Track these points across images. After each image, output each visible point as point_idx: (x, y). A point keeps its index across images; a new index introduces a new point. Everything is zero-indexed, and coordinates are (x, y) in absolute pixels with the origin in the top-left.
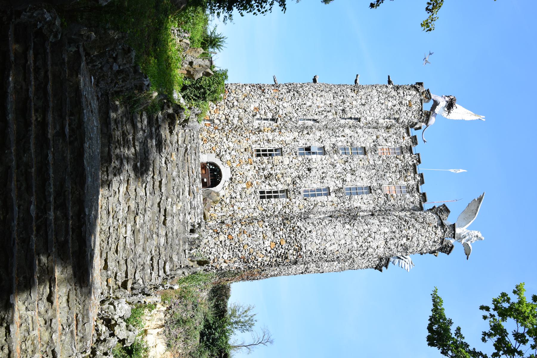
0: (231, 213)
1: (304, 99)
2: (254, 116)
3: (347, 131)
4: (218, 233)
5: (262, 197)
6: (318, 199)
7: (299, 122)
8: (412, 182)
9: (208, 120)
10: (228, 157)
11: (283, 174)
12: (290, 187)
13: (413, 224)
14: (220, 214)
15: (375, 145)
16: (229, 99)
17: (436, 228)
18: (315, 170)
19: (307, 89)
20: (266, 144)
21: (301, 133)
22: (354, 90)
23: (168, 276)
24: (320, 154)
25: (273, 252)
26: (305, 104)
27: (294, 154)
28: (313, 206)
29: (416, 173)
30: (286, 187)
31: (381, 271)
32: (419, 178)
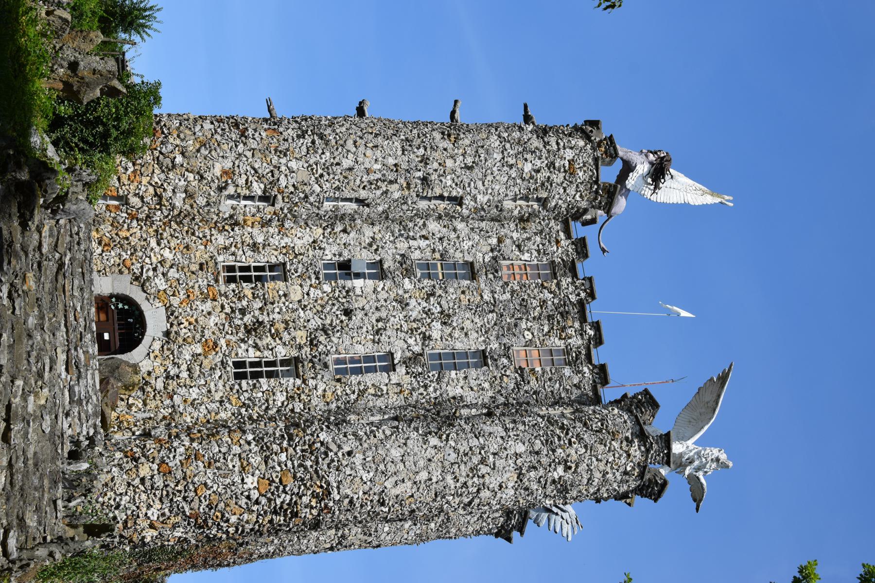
0: (166, 412)
1: (336, 153)
2: (220, 189)
3: (433, 226)
4: (136, 460)
5: (239, 376)
6: (369, 379)
7: (326, 203)
8: (576, 341)
9: (113, 198)
10: (160, 283)
11: (286, 323)
12: (303, 352)
13: (578, 435)
14: (140, 416)
15: (494, 258)
16: (164, 150)
17: (630, 442)
18: (360, 314)
19: (344, 129)
20: (249, 253)
21: (329, 230)
22: (449, 135)
23: (13, 562)
24: (372, 277)
25: (263, 501)
26: (338, 164)
27: (313, 277)
28: (356, 396)
29: (585, 321)
31: (509, 540)
32: (592, 333)
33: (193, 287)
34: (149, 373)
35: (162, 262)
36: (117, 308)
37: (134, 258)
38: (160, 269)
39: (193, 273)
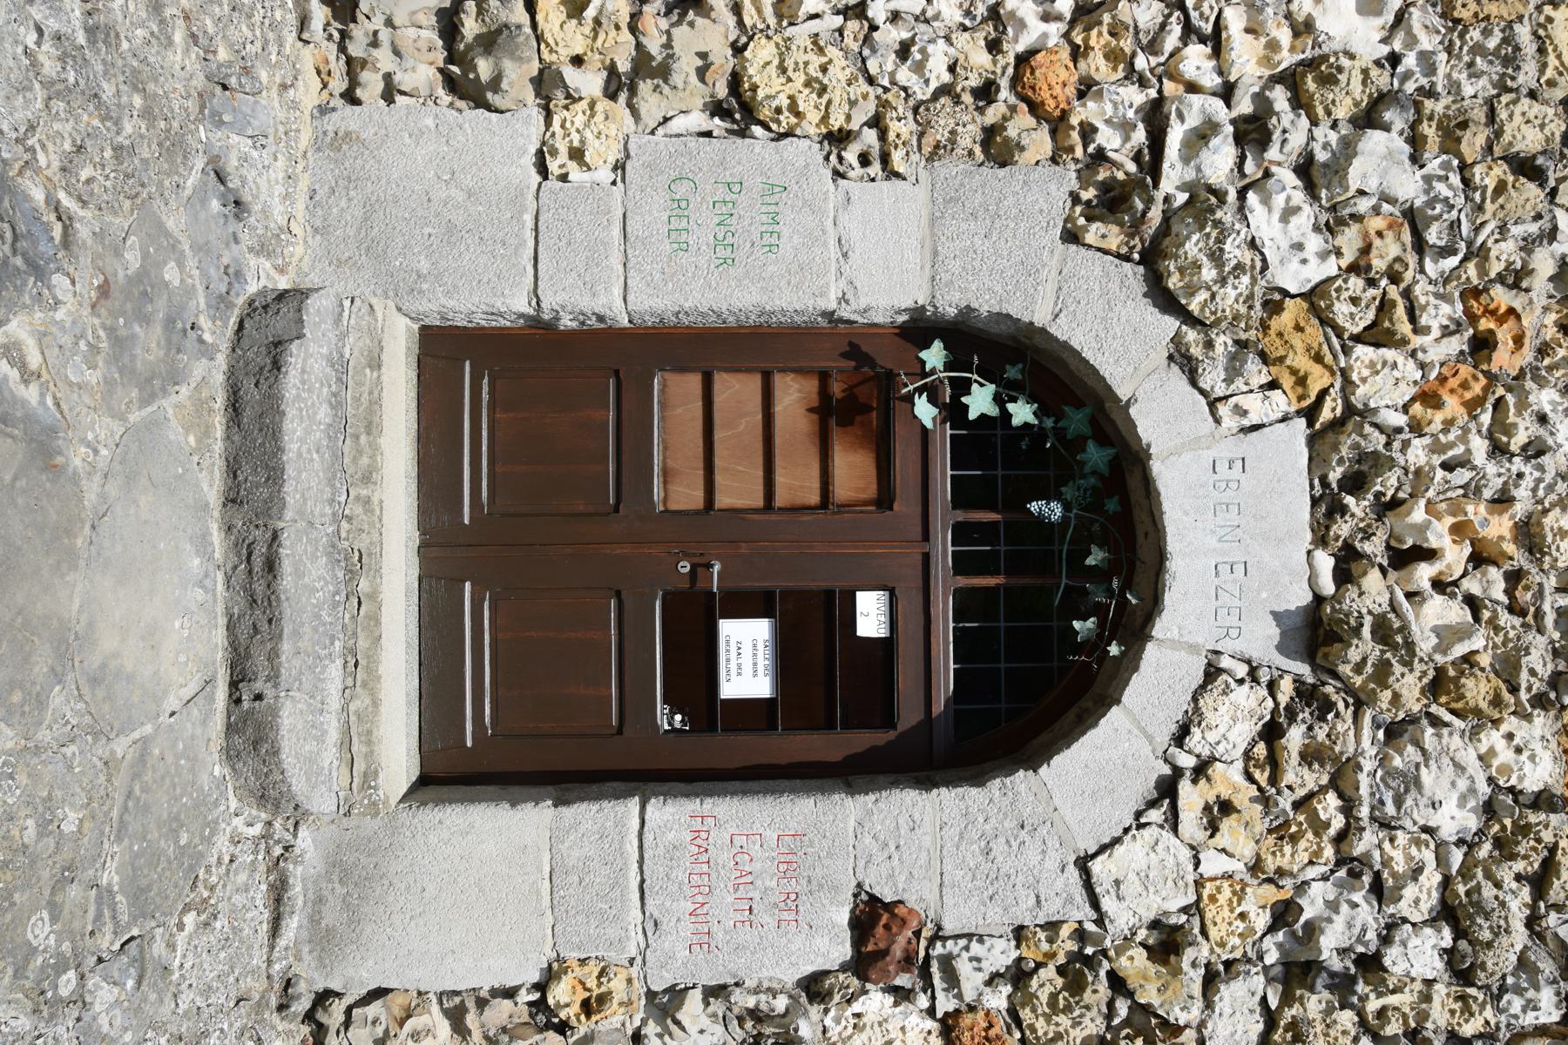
33: (1516, 278)
34: (1167, 943)
35: (1307, 77)
36: (954, 412)
37: (1099, 39)
38: (1293, 133)
39: (1526, 168)
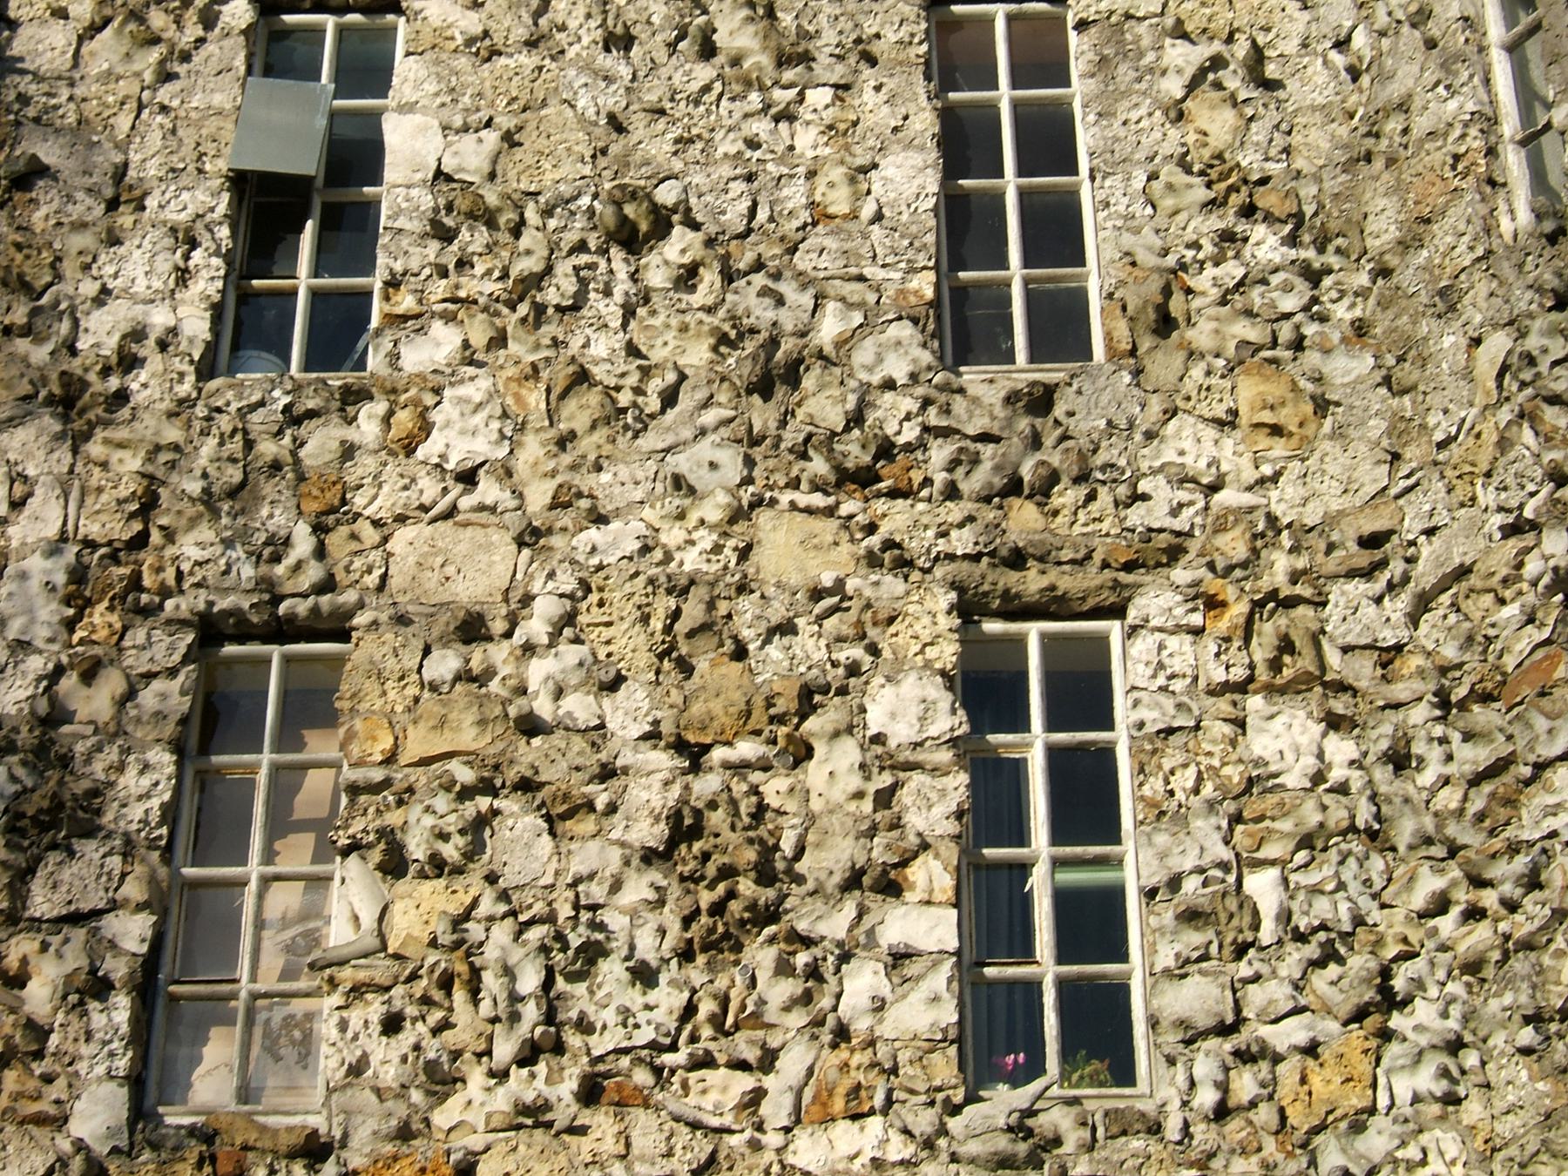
30: (928, 622)
